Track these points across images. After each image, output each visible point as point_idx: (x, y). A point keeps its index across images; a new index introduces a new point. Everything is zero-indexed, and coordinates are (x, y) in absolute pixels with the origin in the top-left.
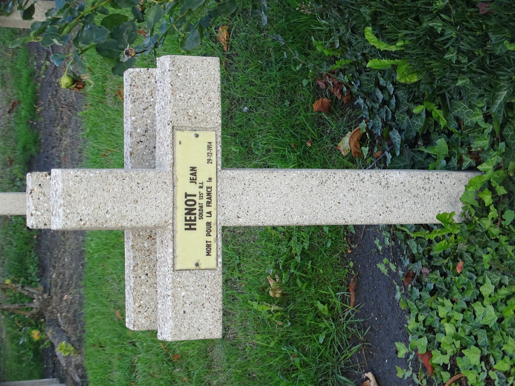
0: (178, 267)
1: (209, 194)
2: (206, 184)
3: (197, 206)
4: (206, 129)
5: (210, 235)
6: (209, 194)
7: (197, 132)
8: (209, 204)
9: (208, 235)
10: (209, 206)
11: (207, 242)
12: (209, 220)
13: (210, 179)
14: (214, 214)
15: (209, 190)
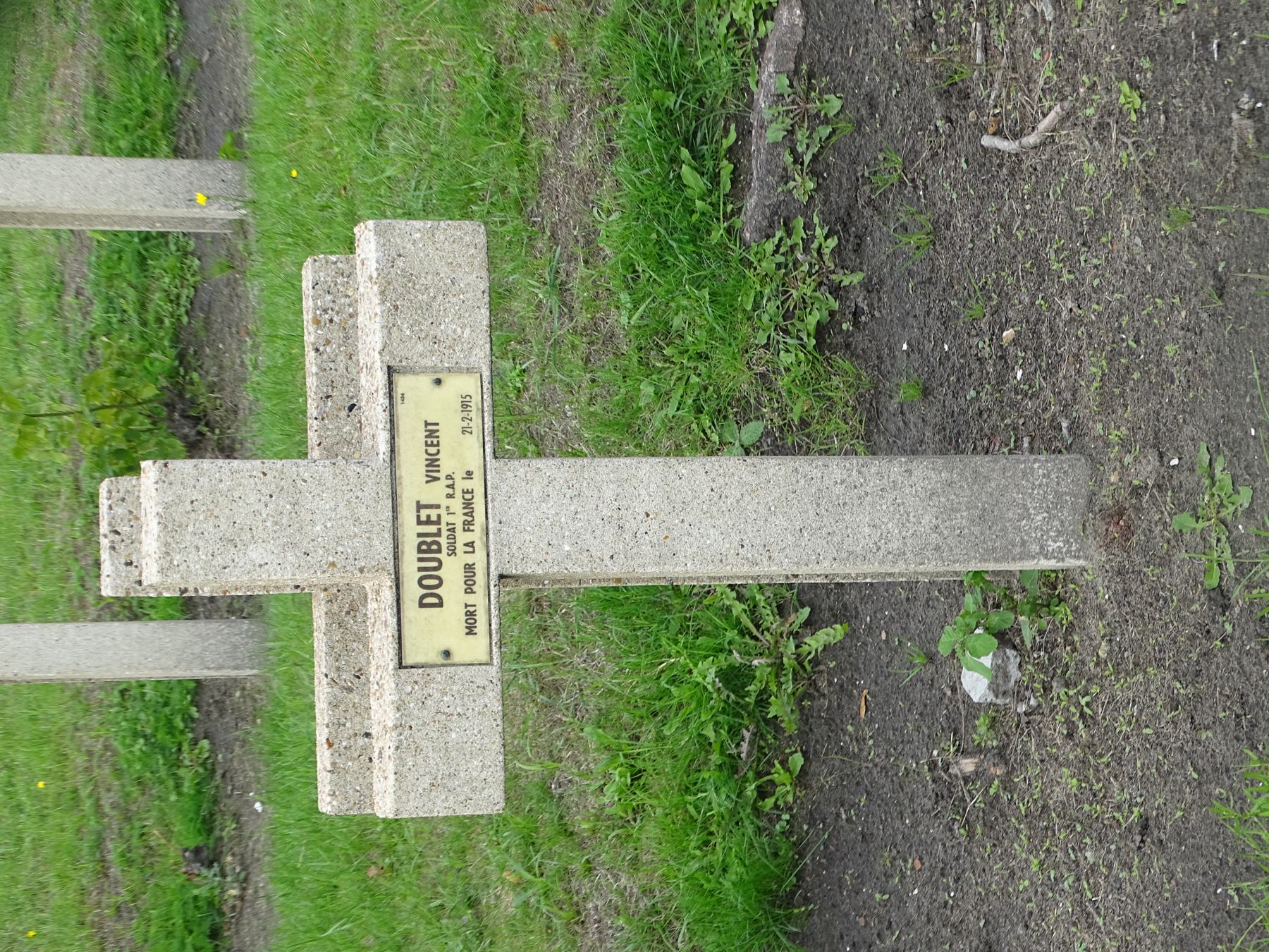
0: (408, 660)
1: (468, 505)
2: (461, 485)
3: (445, 533)
4: (455, 370)
5: (473, 592)
6: (468, 505)
7: (440, 376)
8: (468, 526)
9: (469, 590)
10: (469, 530)
11: (466, 606)
12: (469, 559)
13: (469, 474)
14: (479, 545)
15: (468, 496)
